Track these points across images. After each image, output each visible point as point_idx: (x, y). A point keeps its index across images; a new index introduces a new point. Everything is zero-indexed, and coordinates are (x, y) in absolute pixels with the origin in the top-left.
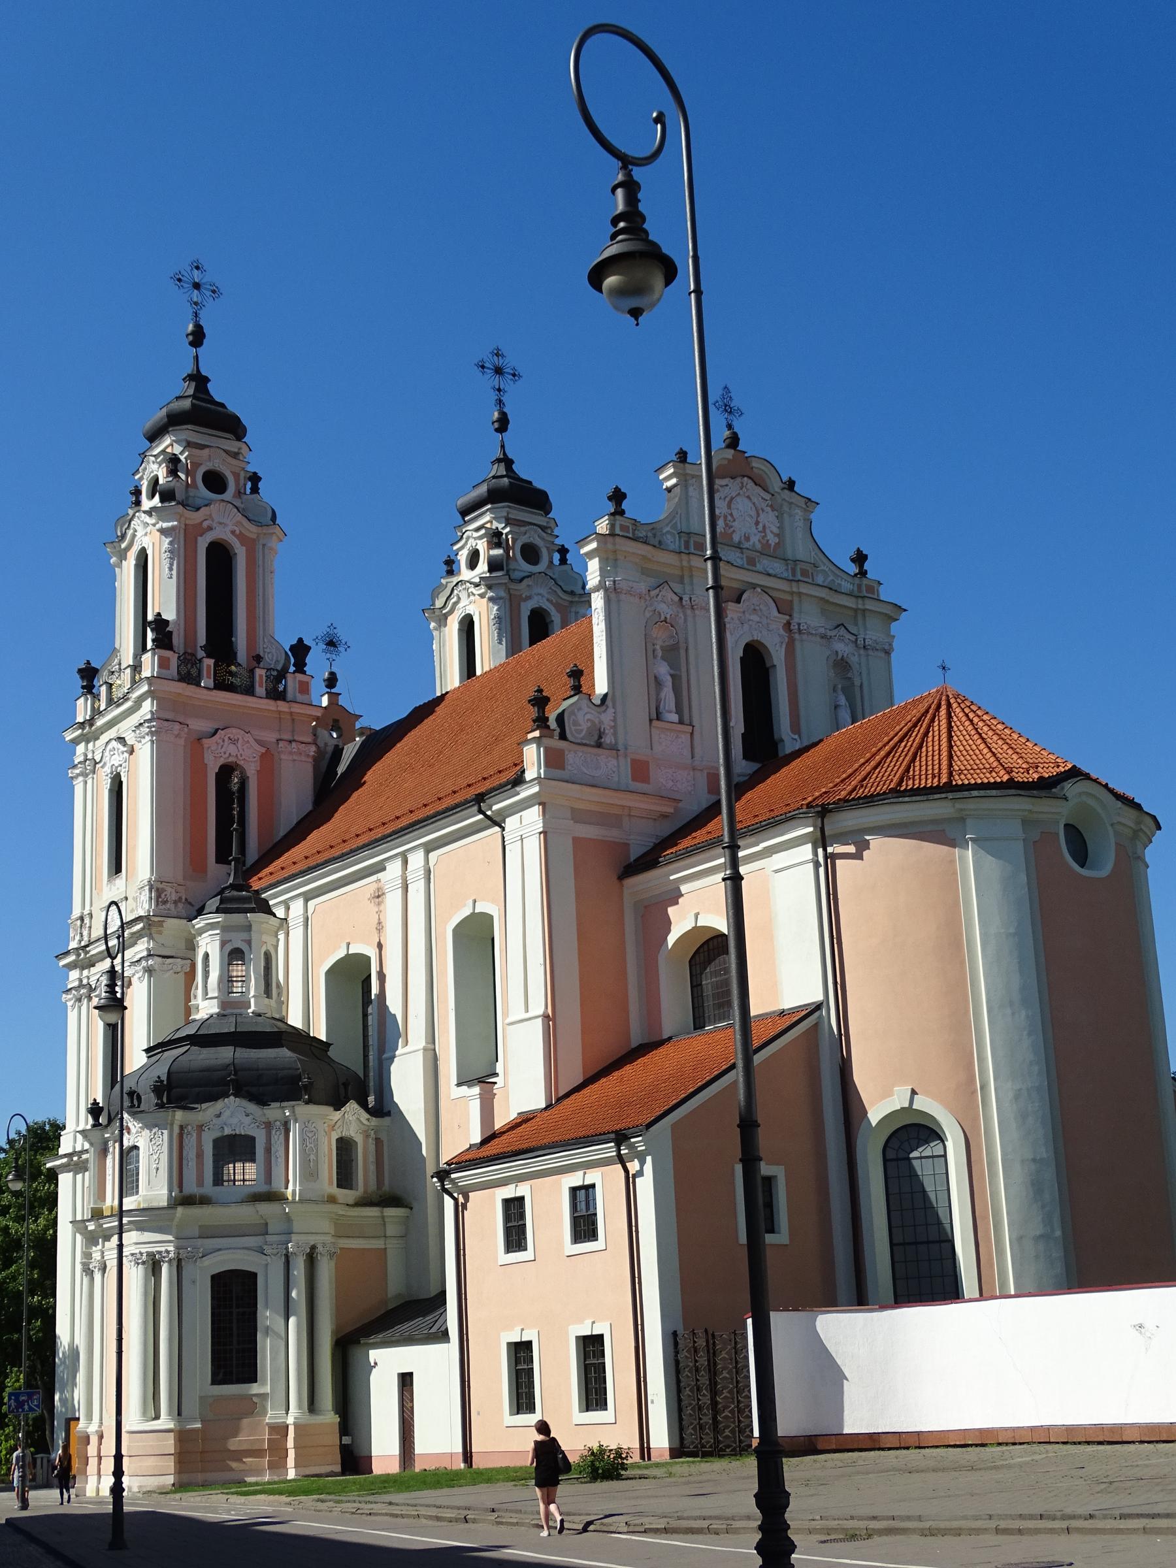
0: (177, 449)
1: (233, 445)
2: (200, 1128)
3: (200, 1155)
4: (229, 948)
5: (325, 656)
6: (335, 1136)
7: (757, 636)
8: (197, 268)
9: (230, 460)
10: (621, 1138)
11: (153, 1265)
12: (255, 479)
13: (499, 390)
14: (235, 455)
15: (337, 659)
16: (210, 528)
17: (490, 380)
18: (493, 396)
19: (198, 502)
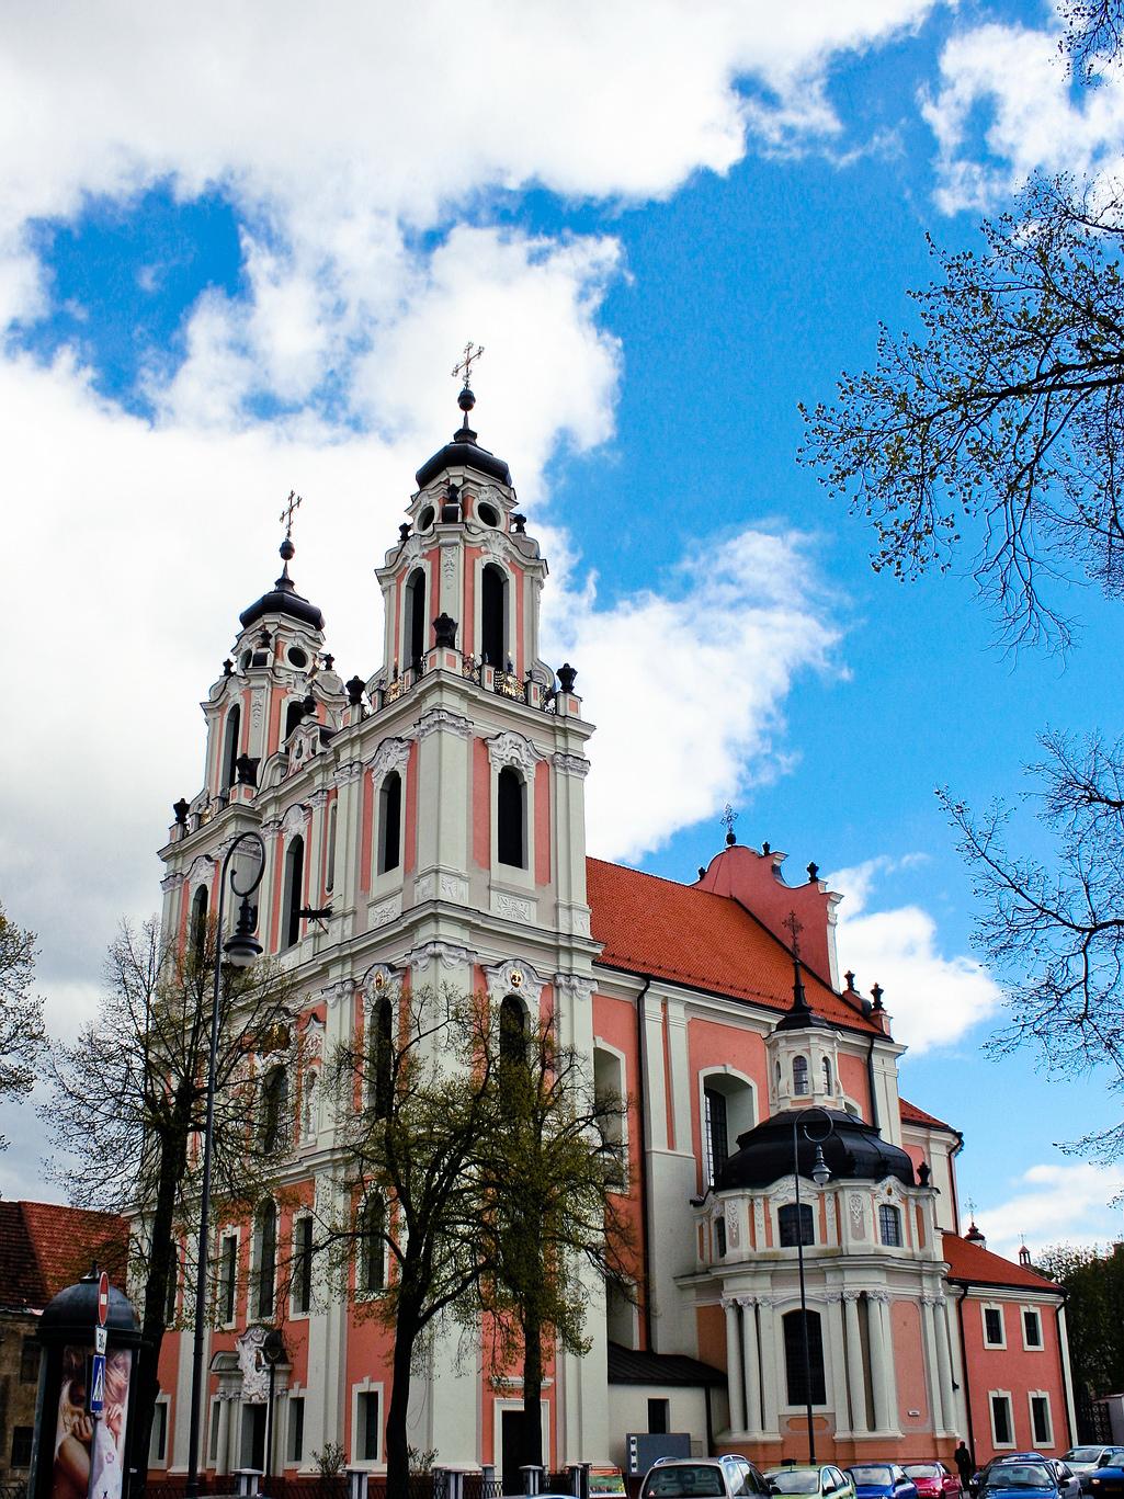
2: (766, 1199)
3: (768, 1221)
4: (793, 1056)
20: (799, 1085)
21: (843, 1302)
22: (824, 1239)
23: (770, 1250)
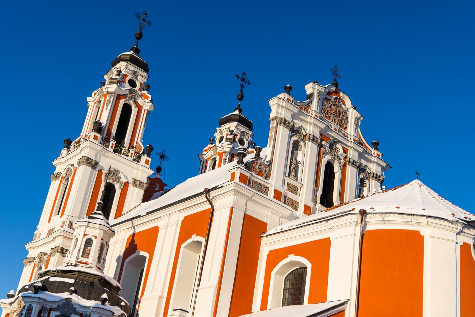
5: (159, 161)
8: (145, 14)
13: (242, 86)
15: (163, 163)
17: (239, 82)
18: (240, 87)
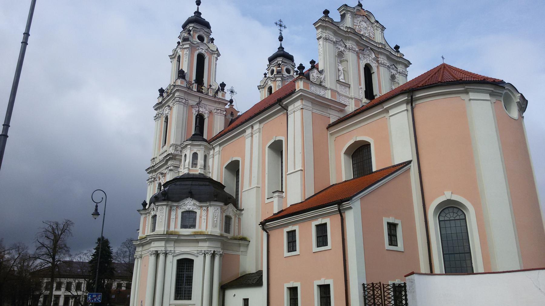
0: (191, 28)
1: (207, 30)
2: (177, 207)
3: (176, 218)
6: (224, 215)
7: (368, 62)
9: (205, 33)
10: (339, 203)
11: (157, 254)
12: (212, 40)
14: (207, 32)
16: (198, 49)
17: (278, 28)
18: (279, 31)
19: (195, 43)
20: (194, 164)
21: (205, 254)
22: (200, 227)
23: (176, 230)
